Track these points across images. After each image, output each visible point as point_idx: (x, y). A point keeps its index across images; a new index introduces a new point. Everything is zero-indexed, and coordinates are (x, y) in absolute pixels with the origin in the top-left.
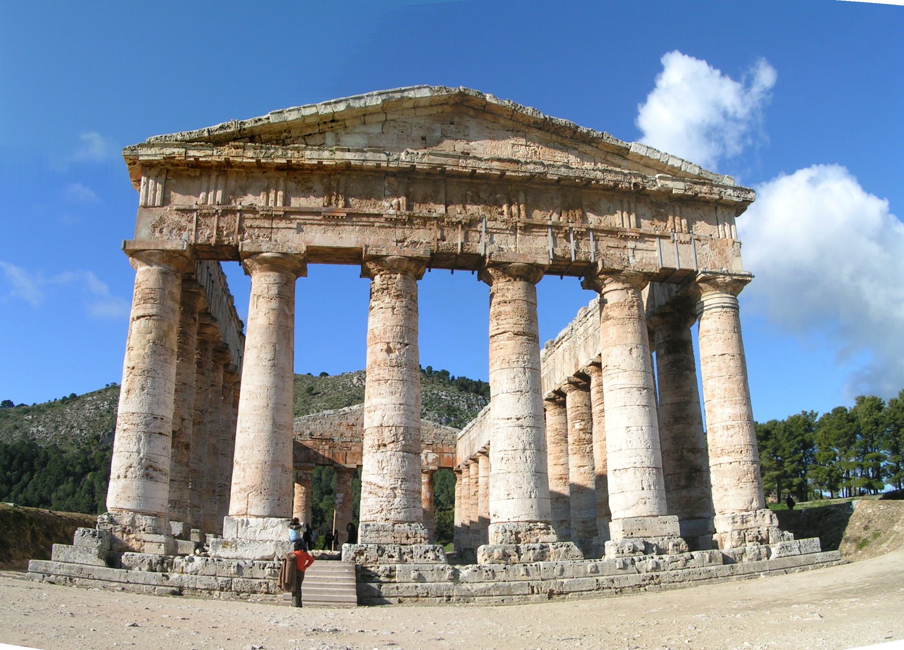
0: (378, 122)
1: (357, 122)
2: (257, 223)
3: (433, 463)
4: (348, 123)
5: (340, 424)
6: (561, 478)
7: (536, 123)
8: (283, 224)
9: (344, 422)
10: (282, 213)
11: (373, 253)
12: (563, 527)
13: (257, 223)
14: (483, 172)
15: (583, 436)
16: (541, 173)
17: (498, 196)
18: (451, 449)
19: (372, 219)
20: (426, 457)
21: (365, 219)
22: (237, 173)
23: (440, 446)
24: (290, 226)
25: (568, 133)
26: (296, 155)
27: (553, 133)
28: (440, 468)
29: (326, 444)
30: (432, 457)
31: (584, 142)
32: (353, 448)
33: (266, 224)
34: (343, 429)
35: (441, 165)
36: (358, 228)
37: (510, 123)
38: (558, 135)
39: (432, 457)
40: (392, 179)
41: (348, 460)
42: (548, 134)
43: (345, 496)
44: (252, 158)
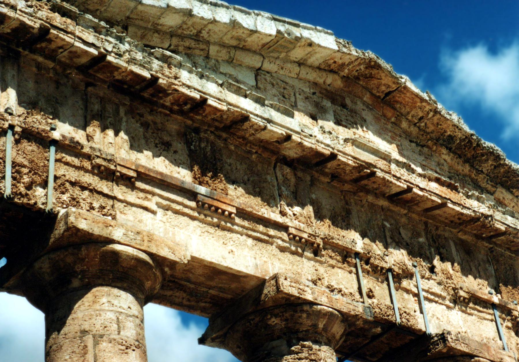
0: (250, 68)
1: (224, 54)
2: (88, 179)
4: (213, 50)
7: (451, 138)
8: (132, 197)
10: (132, 174)
11: (294, 292)
13: (88, 179)
14: (421, 193)
16: (486, 217)
17: (421, 240)
19: (272, 232)
21: (261, 228)
22: (39, 66)
24: (146, 204)
25: (487, 166)
26: (167, 71)
27: (467, 161)
31: (503, 185)
33: (104, 187)
35: (370, 165)
36: (250, 241)
37: (414, 130)
38: (472, 166)
40: (287, 170)
42: (461, 161)
44: (92, 45)
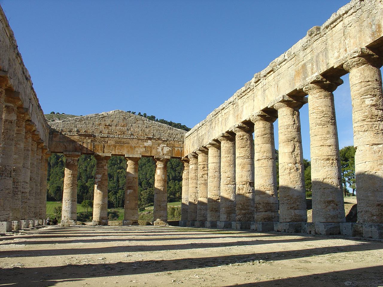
3: (167, 154)
5: (100, 124)
6: (328, 159)
9: (103, 123)
12: (330, 207)
15: (375, 112)
18: (180, 145)
20: (162, 150)
23: (172, 142)
28: (172, 157)
29: (89, 139)
30: (166, 149)
32: (109, 142)
34: (102, 128)
39: (166, 149)
41: (105, 151)
43: (103, 177)
